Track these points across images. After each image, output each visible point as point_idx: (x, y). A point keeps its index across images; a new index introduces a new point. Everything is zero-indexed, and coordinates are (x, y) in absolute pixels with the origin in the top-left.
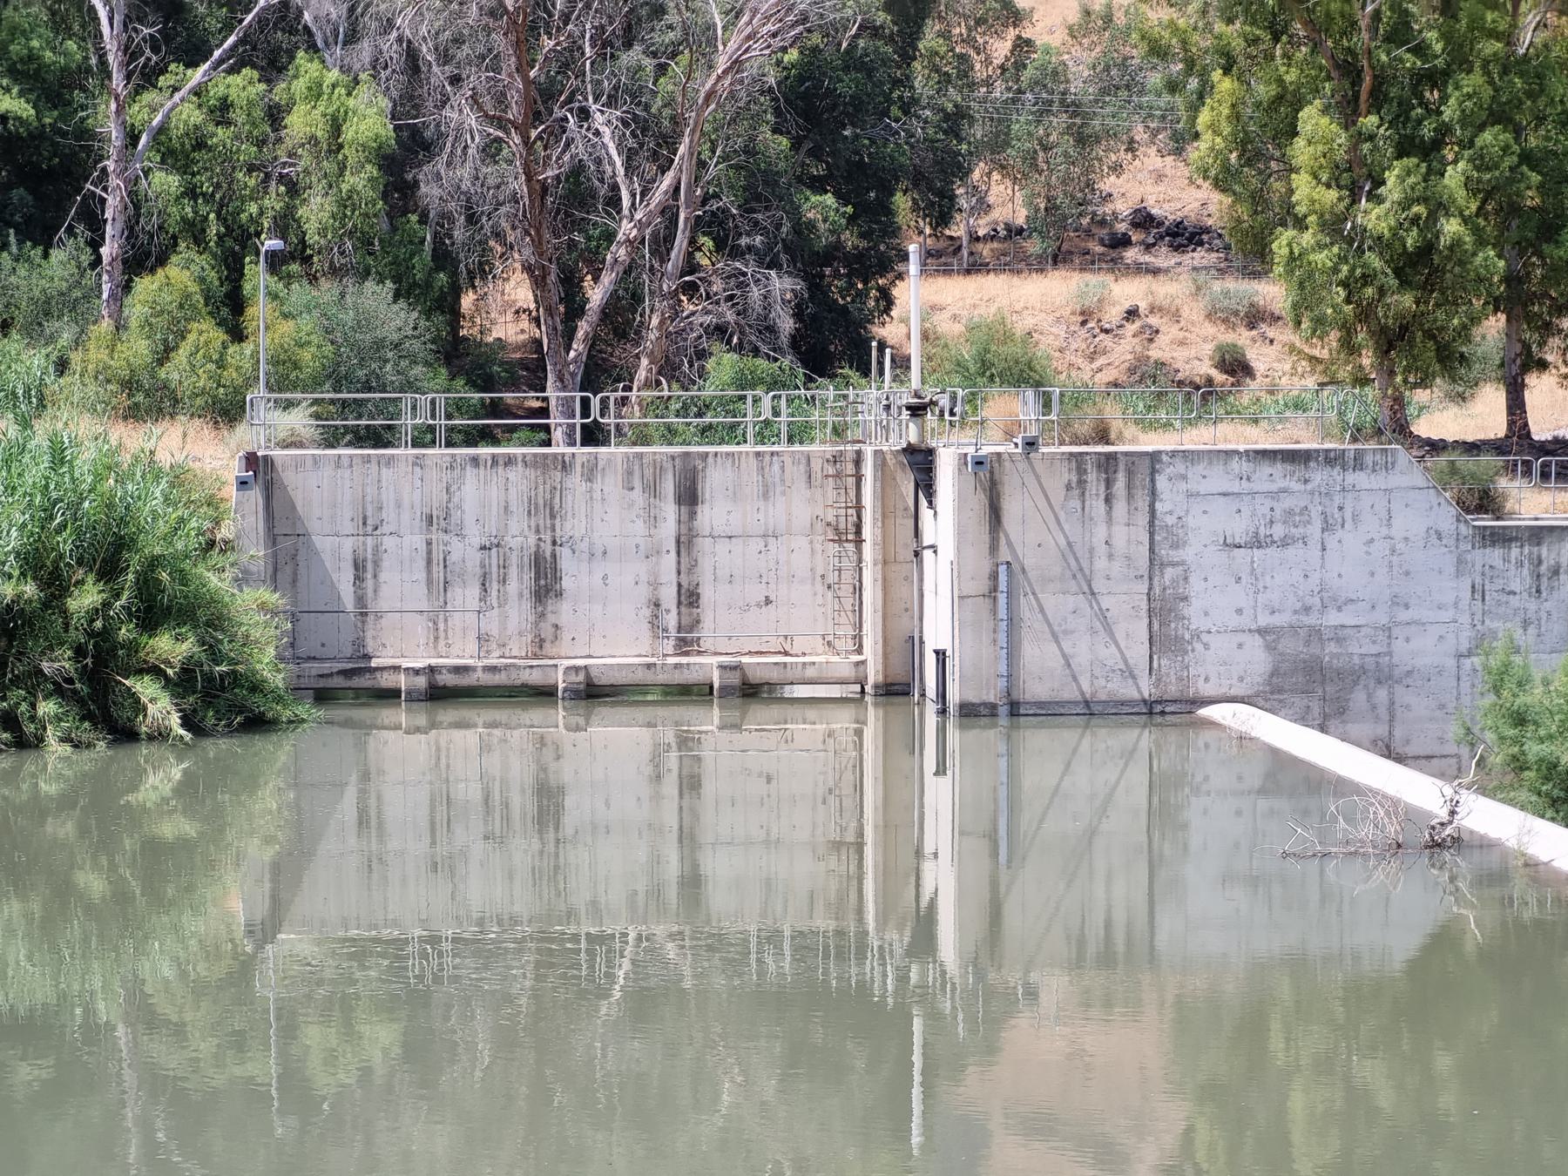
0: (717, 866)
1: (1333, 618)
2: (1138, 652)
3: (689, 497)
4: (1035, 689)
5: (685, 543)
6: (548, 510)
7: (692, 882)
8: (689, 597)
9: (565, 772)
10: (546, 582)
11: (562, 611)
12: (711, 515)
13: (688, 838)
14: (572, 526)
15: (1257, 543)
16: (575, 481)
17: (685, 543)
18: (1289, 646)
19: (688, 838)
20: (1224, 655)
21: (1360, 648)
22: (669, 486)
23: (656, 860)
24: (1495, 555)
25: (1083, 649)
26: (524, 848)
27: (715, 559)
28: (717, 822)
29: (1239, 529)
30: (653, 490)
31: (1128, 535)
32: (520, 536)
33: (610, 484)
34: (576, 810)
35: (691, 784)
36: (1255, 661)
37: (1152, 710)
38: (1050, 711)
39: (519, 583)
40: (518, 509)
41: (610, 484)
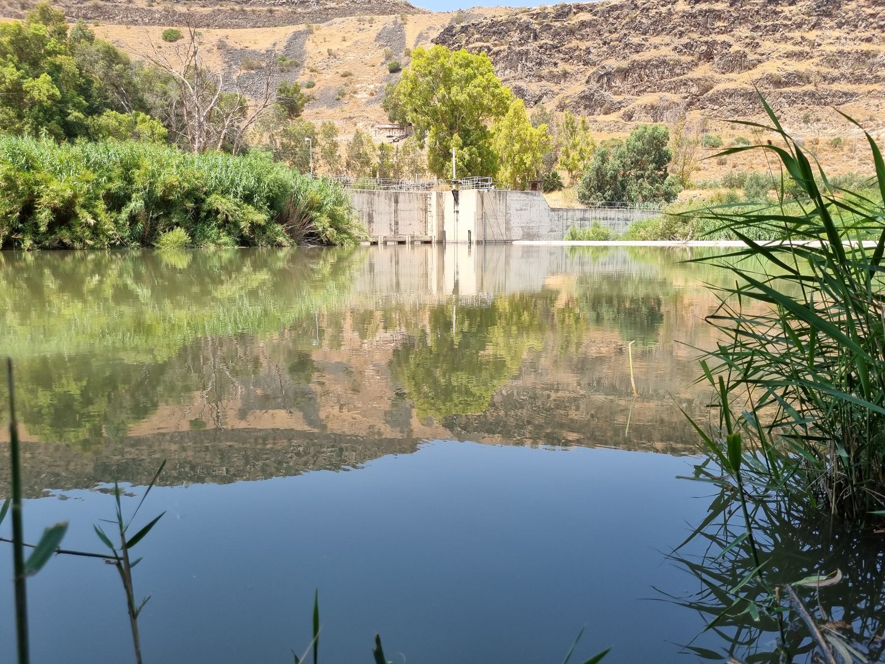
0: (402, 281)
1: (532, 225)
2: (503, 231)
3: (396, 202)
4: (489, 238)
5: (396, 211)
6: (371, 203)
7: (398, 284)
8: (397, 223)
9: (375, 261)
10: (371, 220)
11: (374, 226)
12: (401, 206)
13: (397, 274)
14: (375, 207)
15: (521, 210)
16: (376, 197)
17: (396, 211)
18: (525, 230)
19: (397, 274)
20: (516, 233)
21: (535, 230)
22: (393, 199)
23: (391, 279)
24: (553, 213)
25: (496, 230)
26: (367, 277)
27: (401, 214)
28: (402, 271)
29: (518, 207)
30: (390, 200)
31: (503, 208)
32: (366, 209)
33: (382, 198)
34: (377, 268)
35: (397, 263)
36: (520, 233)
37: (505, 242)
38: (491, 242)
39: (366, 219)
40: (365, 203)
41: (382, 198)
